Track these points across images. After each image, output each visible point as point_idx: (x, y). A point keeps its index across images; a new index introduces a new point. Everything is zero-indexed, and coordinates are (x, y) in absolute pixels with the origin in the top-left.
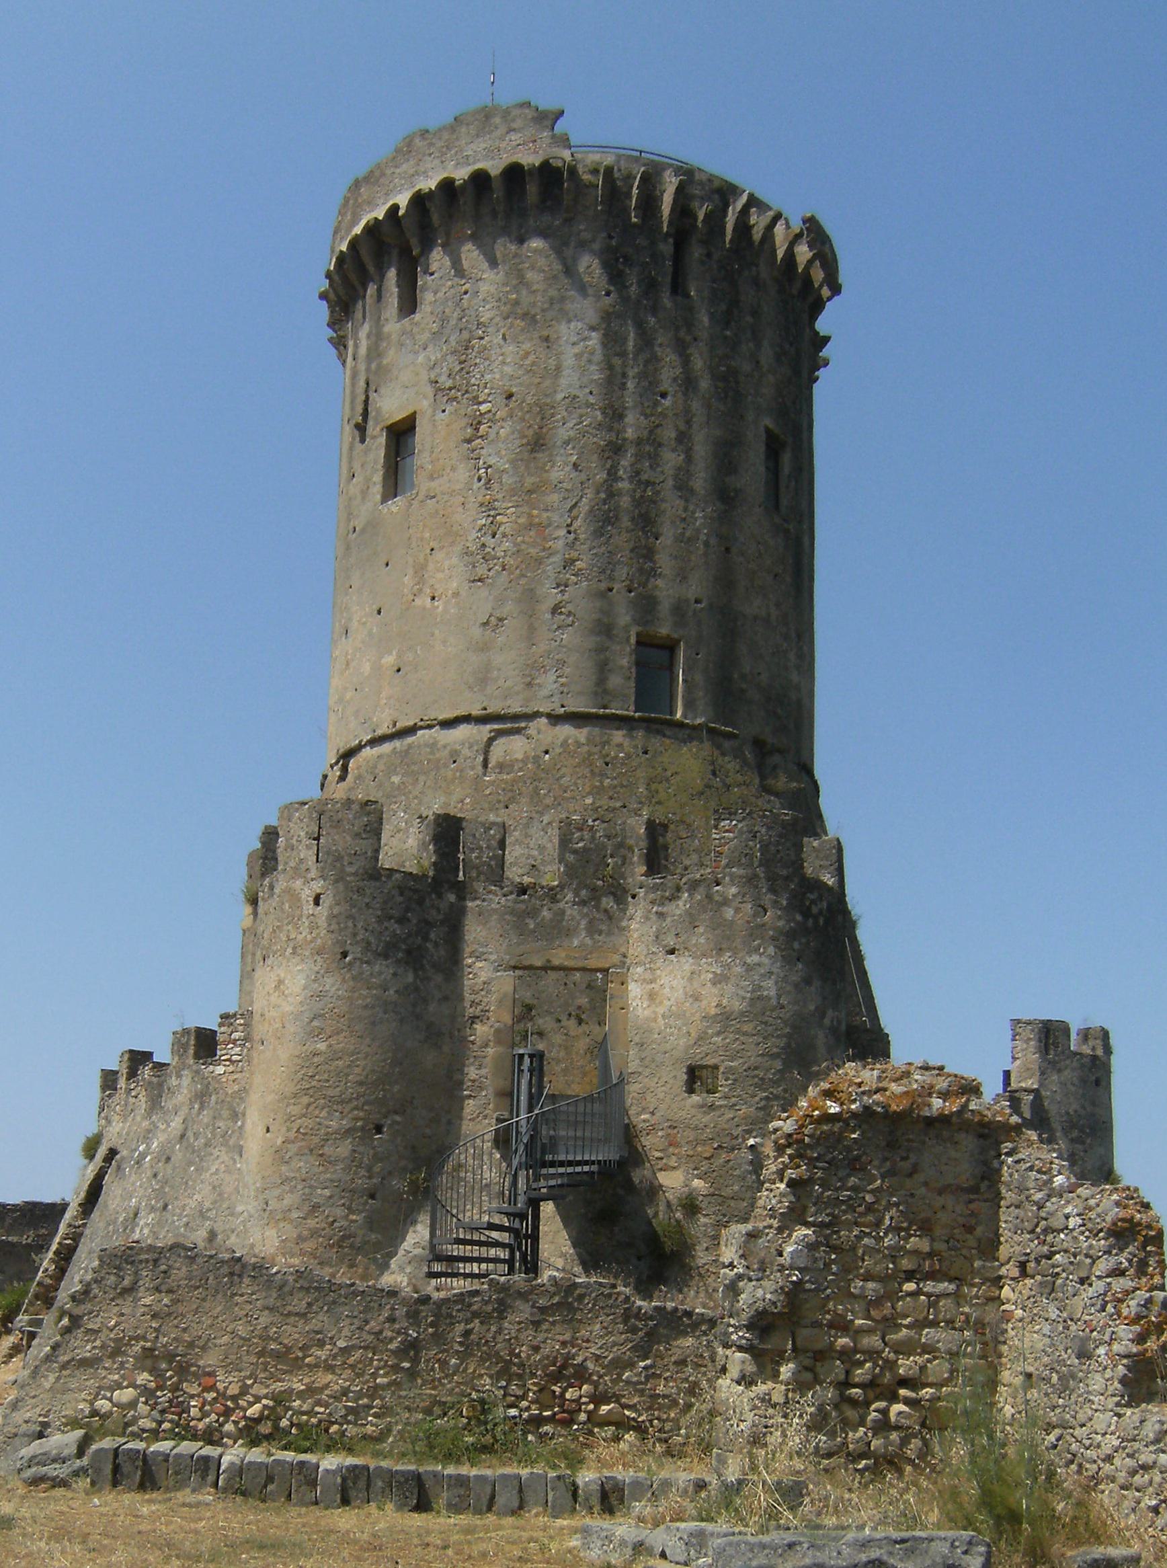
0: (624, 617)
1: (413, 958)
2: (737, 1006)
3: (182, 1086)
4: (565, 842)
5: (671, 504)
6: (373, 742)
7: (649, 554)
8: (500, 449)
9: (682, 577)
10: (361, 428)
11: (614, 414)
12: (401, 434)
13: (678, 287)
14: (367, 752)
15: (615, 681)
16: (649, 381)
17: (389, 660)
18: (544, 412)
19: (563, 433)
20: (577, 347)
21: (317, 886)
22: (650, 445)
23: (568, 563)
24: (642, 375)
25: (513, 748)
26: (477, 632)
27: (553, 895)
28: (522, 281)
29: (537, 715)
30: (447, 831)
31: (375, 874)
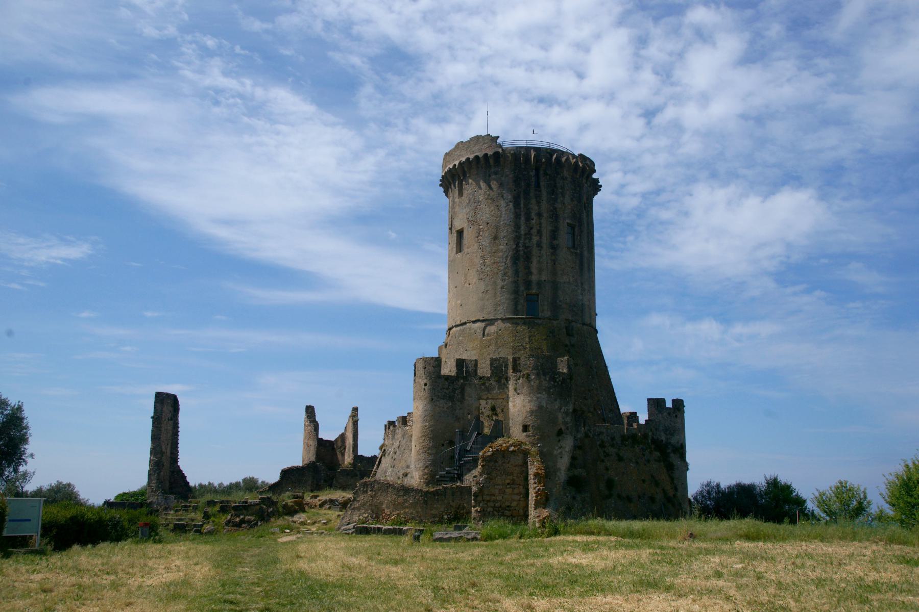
0: (522, 288)
1: (451, 398)
2: (535, 408)
3: (399, 432)
4: (491, 364)
5: (535, 251)
6: (457, 326)
8: (485, 242)
11: (517, 227)
12: (460, 233)
14: (454, 329)
15: (520, 307)
17: (459, 302)
18: (497, 228)
21: (425, 381)
25: (492, 329)
26: (481, 294)
27: (488, 379)
29: (497, 320)
30: (460, 363)
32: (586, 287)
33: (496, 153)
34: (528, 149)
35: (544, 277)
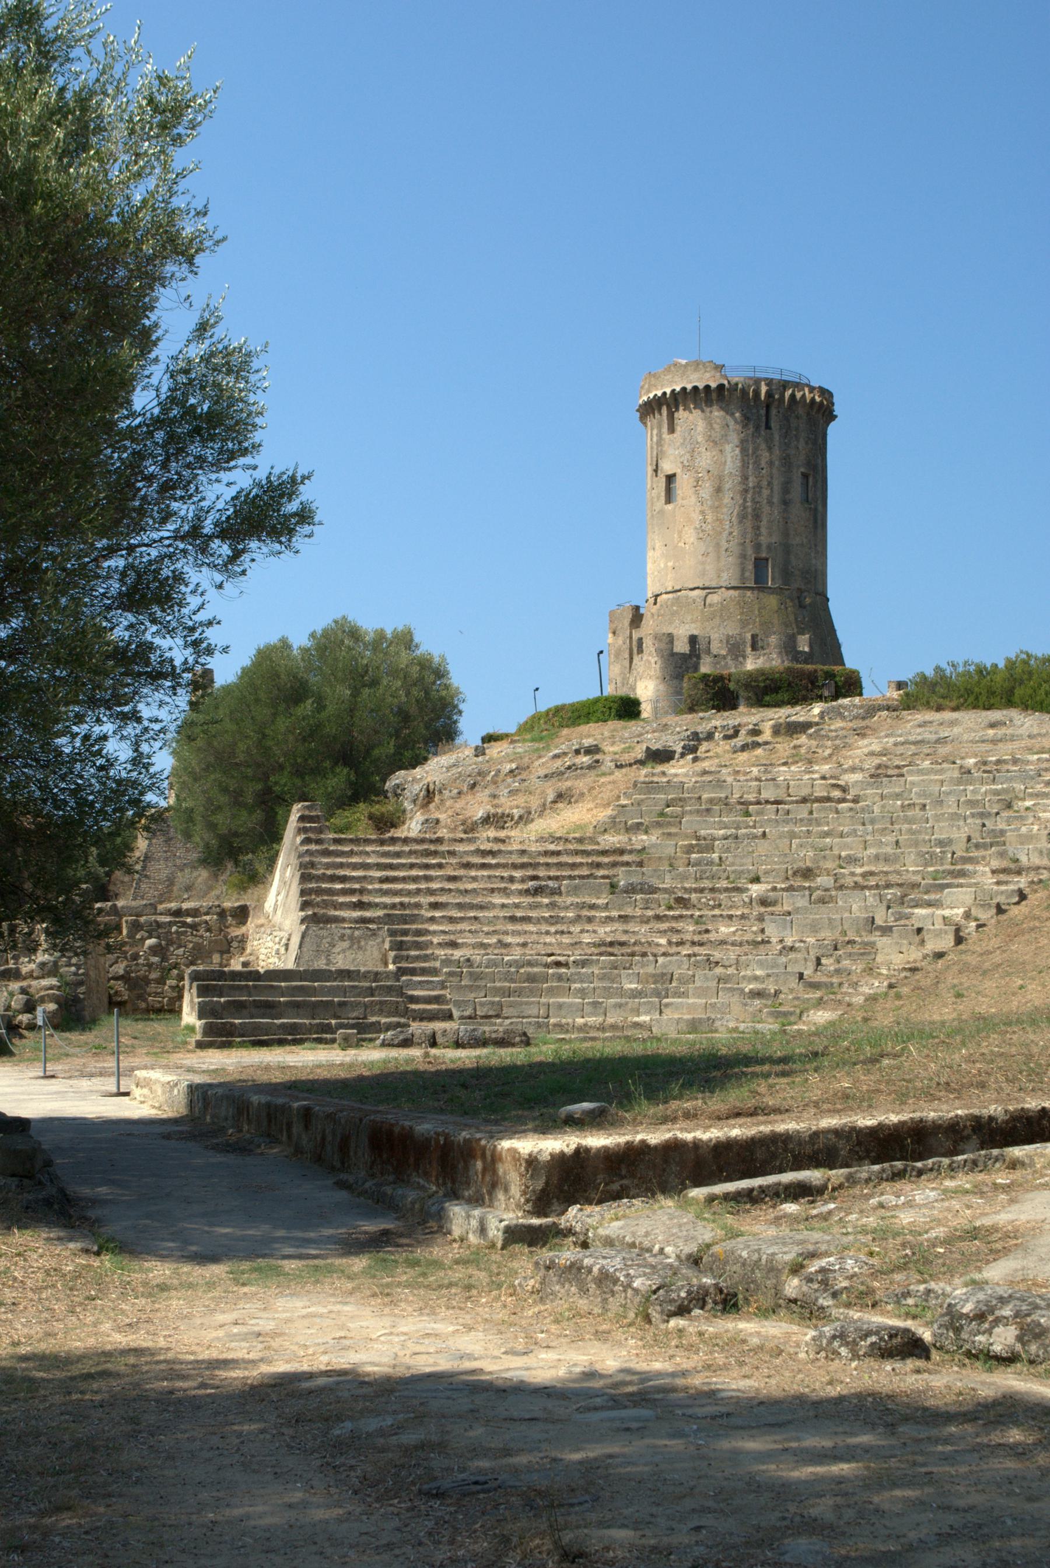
0: (750, 551)
5: (766, 509)
7: (758, 528)
8: (706, 490)
9: (770, 535)
10: (656, 471)
11: (745, 478)
12: (670, 478)
13: (768, 427)
14: (664, 596)
15: (747, 574)
16: (757, 463)
17: (670, 564)
18: (720, 478)
19: (727, 486)
20: (731, 455)
22: (758, 487)
23: (731, 533)
24: (755, 463)
25: (714, 598)
27: (724, 657)
28: (712, 428)
30: (693, 640)
31: (673, 654)
32: (820, 549)
33: (721, 387)
34: (757, 382)
35: (774, 539)
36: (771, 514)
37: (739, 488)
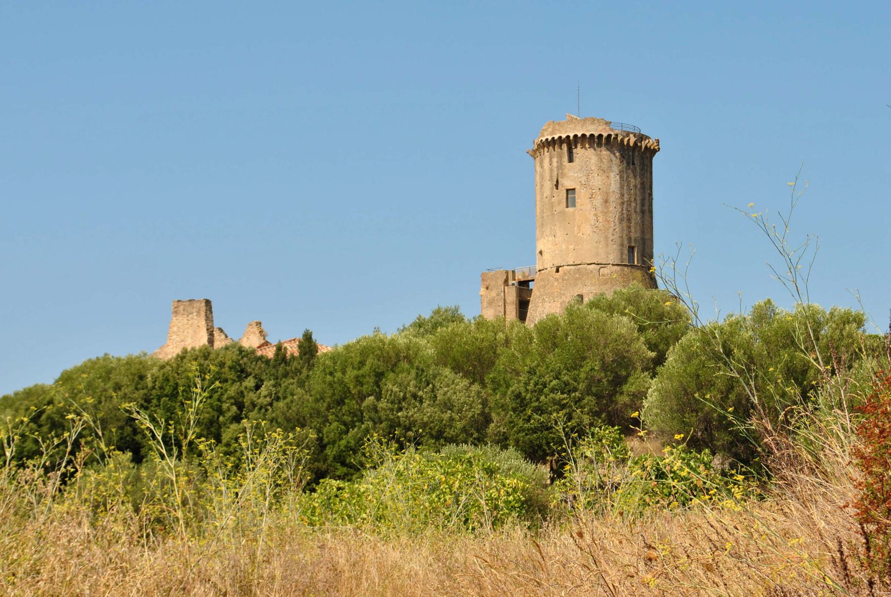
0: (626, 242)
5: (634, 216)
7: (629, 227)
8: (598, 201)
9: (636, 231)
17: (571, 247)
19: (612, 199)
22: (629, 201)
36: (636, 218)
37: (620, 201)
